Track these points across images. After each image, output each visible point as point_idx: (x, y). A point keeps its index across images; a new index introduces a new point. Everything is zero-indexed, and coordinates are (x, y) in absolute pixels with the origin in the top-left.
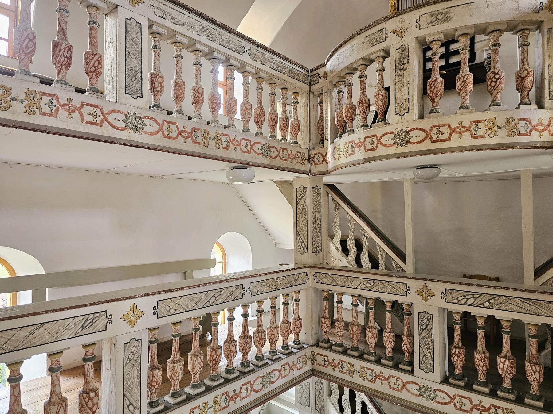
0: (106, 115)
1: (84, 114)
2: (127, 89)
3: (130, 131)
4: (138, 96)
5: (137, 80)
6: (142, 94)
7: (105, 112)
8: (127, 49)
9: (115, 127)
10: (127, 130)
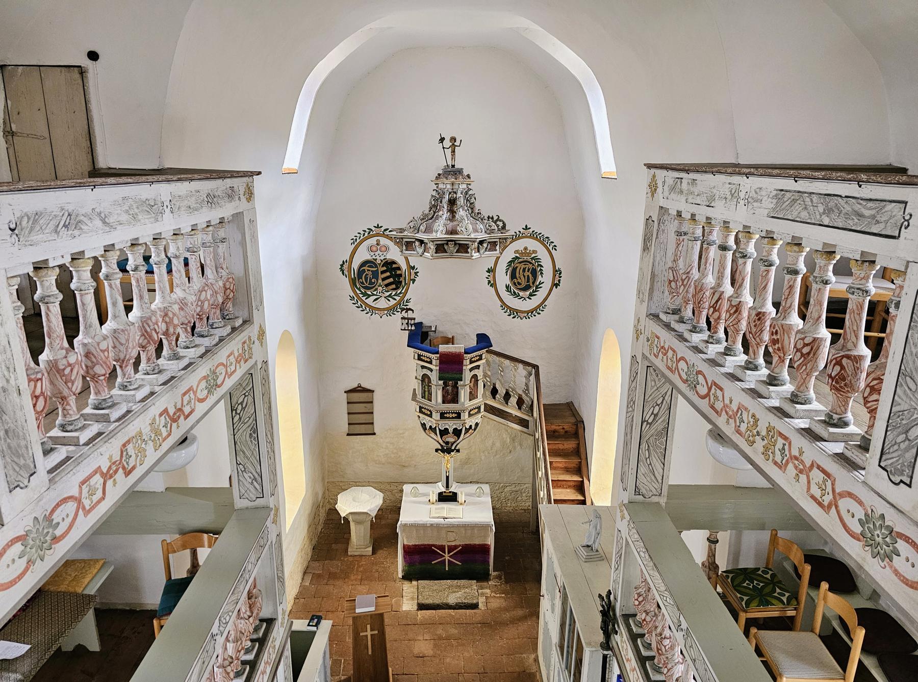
0: (838, 497)
1: (811, 481)
2: (884, 457)
3: (867, 548)
4: (902, 481)
5: (907, 442)
6: (912, 477)
7: (838, 490)
8: (903, 367)
9: (845, 526)
10: (861, 543)
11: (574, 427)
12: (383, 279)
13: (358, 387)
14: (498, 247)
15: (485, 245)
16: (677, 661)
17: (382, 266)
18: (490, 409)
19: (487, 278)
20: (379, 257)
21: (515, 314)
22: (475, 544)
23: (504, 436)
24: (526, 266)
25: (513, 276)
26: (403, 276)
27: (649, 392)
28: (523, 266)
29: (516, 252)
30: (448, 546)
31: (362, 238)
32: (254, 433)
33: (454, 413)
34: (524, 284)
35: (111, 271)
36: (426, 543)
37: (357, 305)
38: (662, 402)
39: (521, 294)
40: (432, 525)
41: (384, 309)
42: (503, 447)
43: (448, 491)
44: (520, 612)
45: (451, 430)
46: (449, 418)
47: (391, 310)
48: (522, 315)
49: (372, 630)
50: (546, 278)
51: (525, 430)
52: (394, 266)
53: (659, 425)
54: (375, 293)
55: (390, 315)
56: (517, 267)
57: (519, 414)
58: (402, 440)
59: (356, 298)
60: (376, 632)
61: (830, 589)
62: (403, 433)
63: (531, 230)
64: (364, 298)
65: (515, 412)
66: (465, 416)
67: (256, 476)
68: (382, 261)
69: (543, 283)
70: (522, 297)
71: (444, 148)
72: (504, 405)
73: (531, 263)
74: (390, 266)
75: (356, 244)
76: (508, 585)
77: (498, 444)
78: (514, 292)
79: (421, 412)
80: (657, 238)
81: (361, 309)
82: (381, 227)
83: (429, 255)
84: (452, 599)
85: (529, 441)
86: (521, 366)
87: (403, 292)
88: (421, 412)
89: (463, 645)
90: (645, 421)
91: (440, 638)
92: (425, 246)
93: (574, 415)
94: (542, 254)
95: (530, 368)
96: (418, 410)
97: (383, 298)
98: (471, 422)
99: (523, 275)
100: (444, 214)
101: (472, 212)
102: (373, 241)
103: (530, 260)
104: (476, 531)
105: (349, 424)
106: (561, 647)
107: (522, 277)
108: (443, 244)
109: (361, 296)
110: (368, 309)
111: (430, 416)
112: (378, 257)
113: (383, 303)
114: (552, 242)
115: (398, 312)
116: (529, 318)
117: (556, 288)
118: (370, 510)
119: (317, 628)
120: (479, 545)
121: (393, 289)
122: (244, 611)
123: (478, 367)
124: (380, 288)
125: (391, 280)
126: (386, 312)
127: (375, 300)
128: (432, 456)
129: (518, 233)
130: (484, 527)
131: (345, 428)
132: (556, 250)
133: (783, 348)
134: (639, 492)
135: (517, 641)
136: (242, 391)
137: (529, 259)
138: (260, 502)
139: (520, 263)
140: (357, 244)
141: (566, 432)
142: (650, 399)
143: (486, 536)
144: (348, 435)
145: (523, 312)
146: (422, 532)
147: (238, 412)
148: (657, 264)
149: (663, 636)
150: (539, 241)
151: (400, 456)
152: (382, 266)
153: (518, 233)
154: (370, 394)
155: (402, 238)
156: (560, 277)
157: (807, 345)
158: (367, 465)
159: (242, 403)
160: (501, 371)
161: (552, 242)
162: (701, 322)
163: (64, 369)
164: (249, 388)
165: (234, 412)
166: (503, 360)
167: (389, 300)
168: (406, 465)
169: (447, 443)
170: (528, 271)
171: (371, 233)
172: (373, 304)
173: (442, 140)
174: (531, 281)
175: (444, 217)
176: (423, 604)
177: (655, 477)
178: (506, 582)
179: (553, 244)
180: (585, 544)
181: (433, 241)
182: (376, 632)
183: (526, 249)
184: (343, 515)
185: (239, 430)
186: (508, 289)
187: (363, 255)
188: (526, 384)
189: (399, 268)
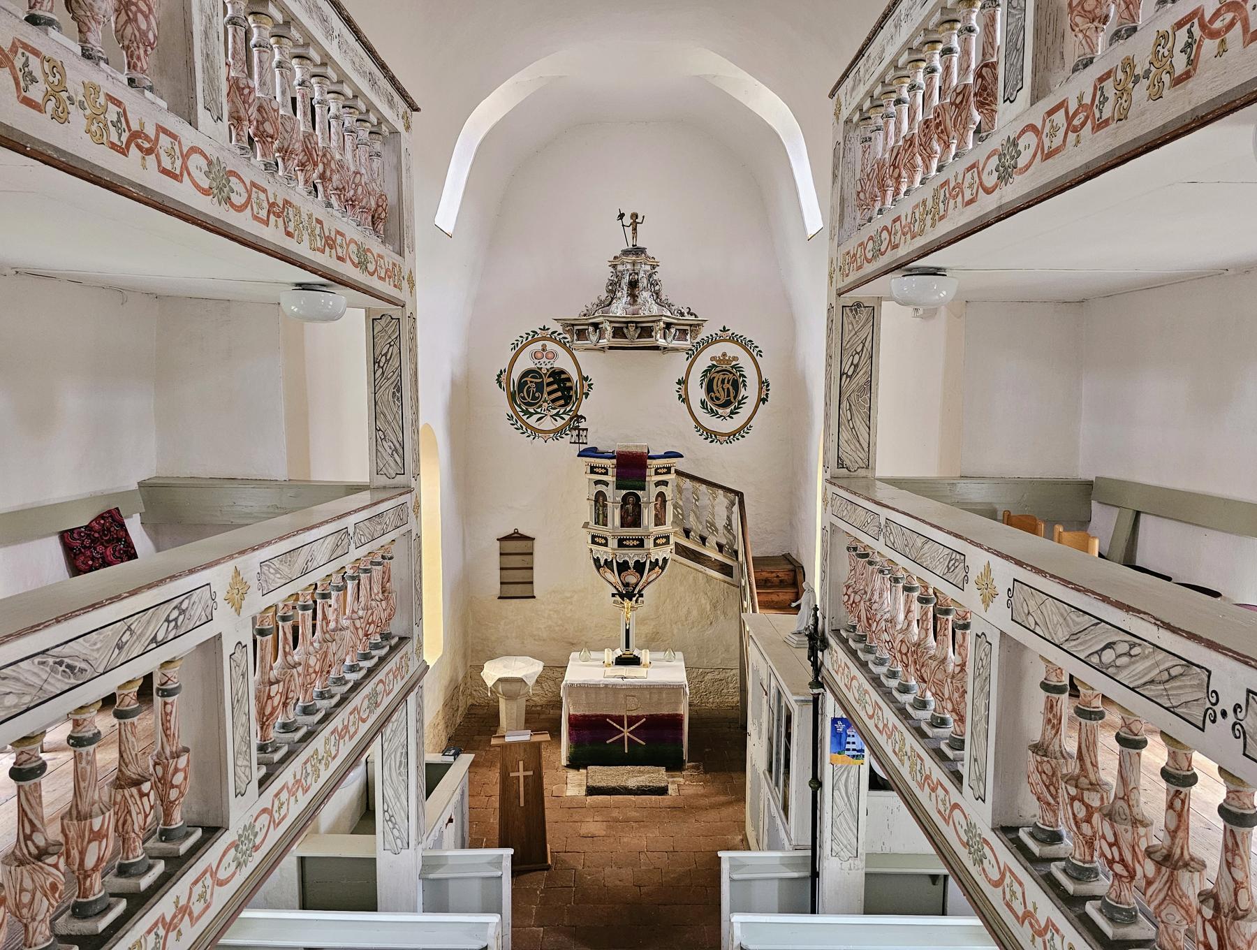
11: (792, 574)
12: (550, 393)
13: (515, 533)
14: (688, 337)
15: (673, 330)
16: (886, 610)
17: (549, 377)
18: (681, 550)
19: (678, 392)
20: (545, 366)
22: (663, 715)
25: (710, 389)
26: (574, 389)
27: (846, 338)
29: (713, 359)
30: (628, 717)
31: (524, 342)
32: (398, 391)
33: (635, 539)
35: (284, 59)
36: (598, 713)
37: (515, 426)
38: (862, 350)
39: (720, 411)
40: (606, 686)
41: (549, 432)
42: (701, 618)
43: (628, 653)
44: (722, 798)
45: (631, 564)
46: (629, 546)
47: (558, 433)
49: (525, 770)
50: (750, 392)
51: (728, 579)
52: (563, 376)
53: (860, 379)
54: (539, 410)
56: (714, 378)
57: (719, 557)
58: (570, 607)
59: (515, 417)
60: (531, 773)
61: (1065, 530)
62: (571, 597)
63: (730, 332)
64: (525, 418)
65: (715, 555)
66: (649, 543)
67: (398, 445)
68: (548, 370)
70: (721, 416)
71: (623, 225)
72: (699, 546)
73: (731, 373)
74: (558, 376)
75: (517, 349)
76: (708, 776)
77: (695, 613)
78: (711, 409)
79: (594, 542)
80: (844, 157)
81: (521, 431)
82: (548, 329)
83: (605, 340)
84: (632, 783)
86: (721, 492)
87: (573, 409)
88: (594, 542)
89: (646, 826)
90: (844, 374)
91: (616, 820)
92: (600, 333)
93: (791, 563)
94: (745, 361)
95: (731, 496)
96: (590, 542)
97: (549, 417)
98: (658, 554)
100: (623, 296)
101: (657, 297)
102: (537, 346)
104: (664, 696)
105: (502, 583)
106: (770, 771)
107: (721, 389)
108: (622, 328)
111: (606, 545)
112: (543, 366)
113: (548, 424)
114: (757, 347)
115: (567, 434)
116: (731, 442)
118: (526, 676)
119: (455, 759)
120: (668, 716)
121: (561, 406)
122: (376, 591)
123: (665, 483)
124: (546, 404)
125: (559, 394)
126: (552, 435)
127: (539, 419)
128: (608, 629)
129: (714, 336)
130: (675, 689)
131: (496, 588)
132: (761, 356)
133: (946, 129)
134: (843, 465)
135: (719, 823)
136: (387, 340)
137: (728, 367)
138: (400, 480)
139: (718, 372)
140: (518, 350)
141: (781, 581)
142: (848, 346)
143: (678, 703)
144: (499, 598)
145: (723, 435)
146: (594, 696)
147: (381, 364)
148: (845, 187)
149: (873, 601)
150: (741, 345)
151: (566, 629)
152: (549, 377)
153: (714, 336)
154: (529, 543)
155: (573, 325)
156: (768, 390)
157: (959, 94)
158: (523, 643)
159: (386, 355)
160: (696, 500)
161: (757, 347)
162: (886, 203)
163: (243, 89)
164: (395, 336)
165: (377, 365)
166: (697, 485)
167: (556, 420)
168: (575, 641)
169: (626, 585)
170: (728, 383)
171: (536, 336)
172: (536, 425)
173: (621, 216)
174: (732, 395)
175: (624, 301)
176: (593, 787)
177: (860, 444)
178: (706, 772)
179: (758, 349)
180: (795, 630)
181: (611, 322)
182: (531, 773)
183: (724, 355)
184: (490, 683)
185: (381, 387)
187: (525, 363)
188: (728, 517)
189: (569, 379)
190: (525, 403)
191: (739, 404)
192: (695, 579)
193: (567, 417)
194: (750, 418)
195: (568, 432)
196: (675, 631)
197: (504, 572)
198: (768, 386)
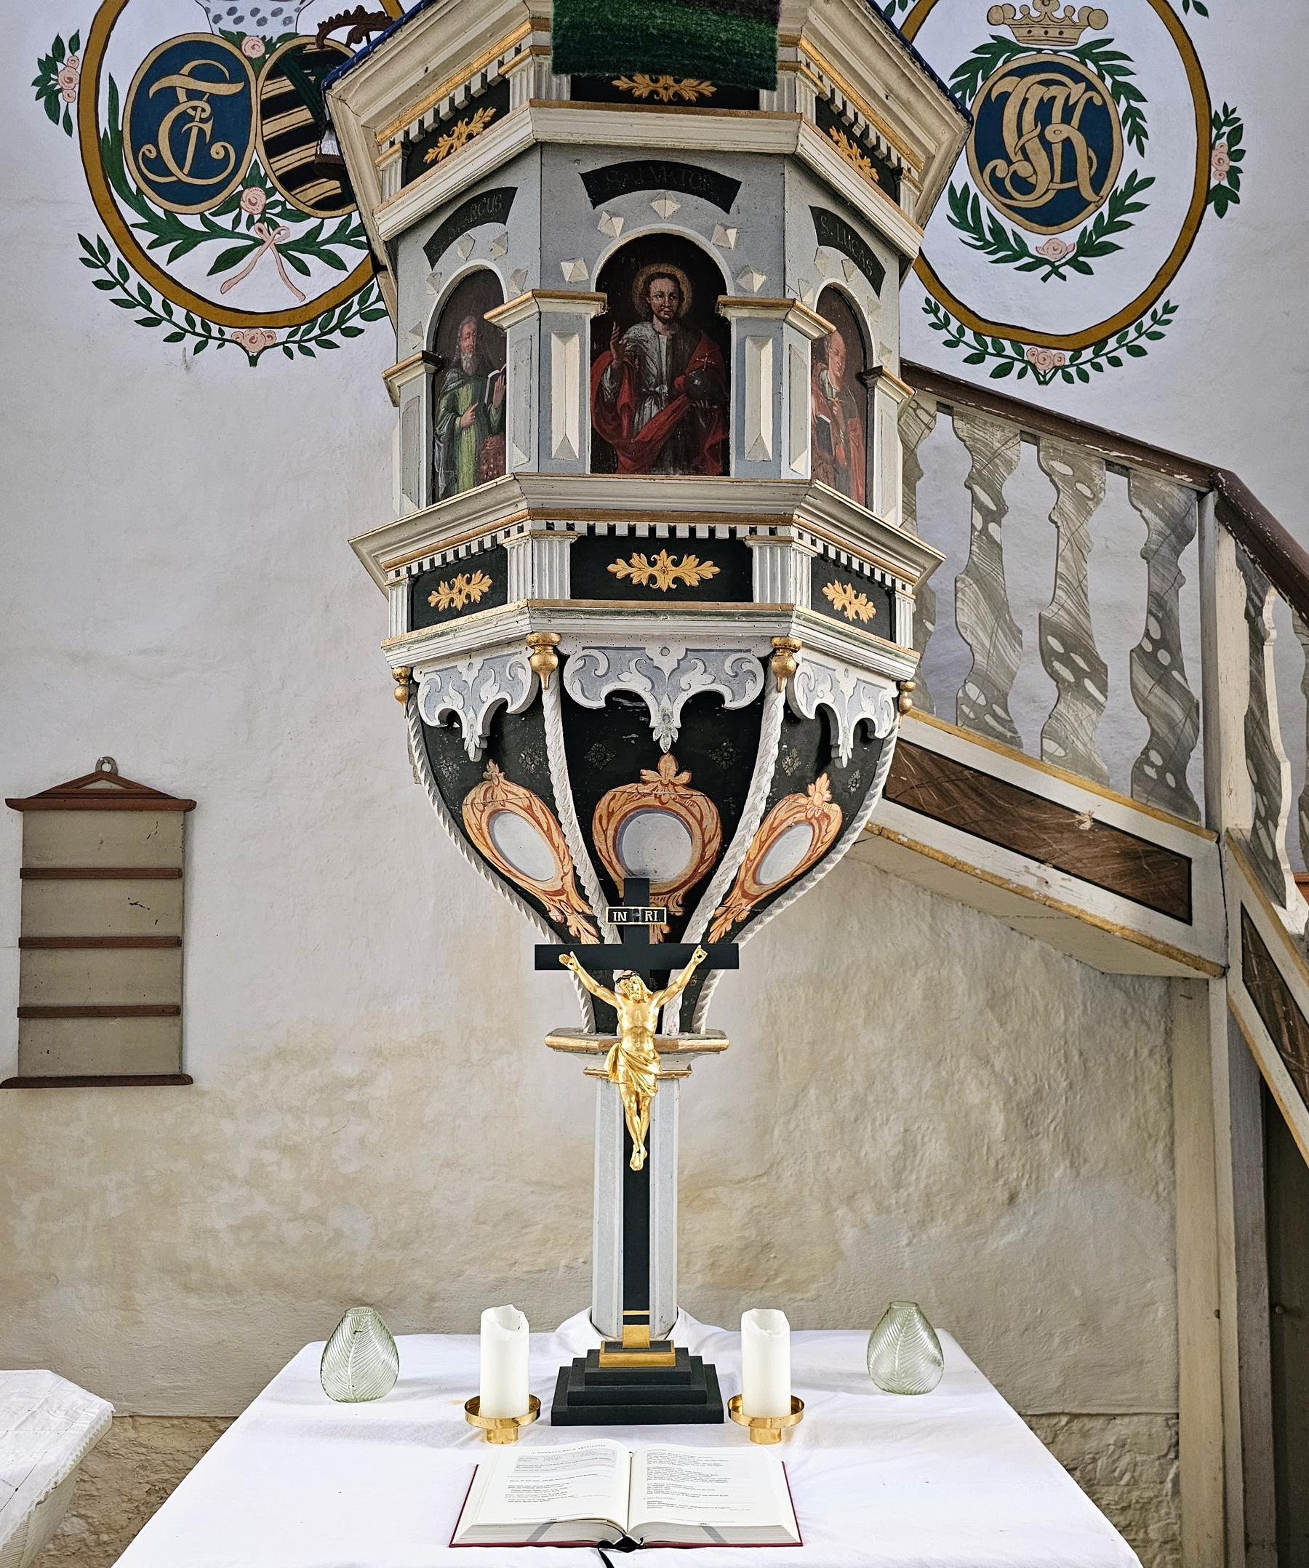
12: (275, 147)
13: (98, 775)
17: (271, 76)
21: (1009, 350)
23: (974, 1096)
24: (1054, 90)
28: (1038, 93)
34: (1046, 187)
39: (1035, 241)
41: (271, 320)
48: (1048, 358)
54: (225, 221)
55: (309, 352)
56: (1005, 96)
59: (115, 254)
68: (270, 46)
69: (1149, 181)
70: (1039, 262)
73: (1077, 77)
77: (935, 1150)
78: (997, 230)
81: (142, 313)
85: (1121, 1128)
97: (268, 255)
99: (1041, 137)
103: (1073, 62)
107: (1034, 147)
109: (144, 238)
110: (179, 314)
112: (249, 26)
116: (1084, 377)
117: (1221, 212)
121: (327, 204)
124: (255, 196)
126: (282, 334)
127: (227, 260)
139: (1022, 72)
151: (339, 1234)
154: (168, 822)
156: (1239, 155)
167: (304, 270)
170: (1066, 119)
172: (210, 289)
186: (962, 216)
190: (158, 189)
191: (1115, 212)
192: (935, 994)
193: (353, 257)
194: (1167, 274)
195: (356, 322)
196: (850, 1235)
197: (38, 955)
198: (1236, 135)
